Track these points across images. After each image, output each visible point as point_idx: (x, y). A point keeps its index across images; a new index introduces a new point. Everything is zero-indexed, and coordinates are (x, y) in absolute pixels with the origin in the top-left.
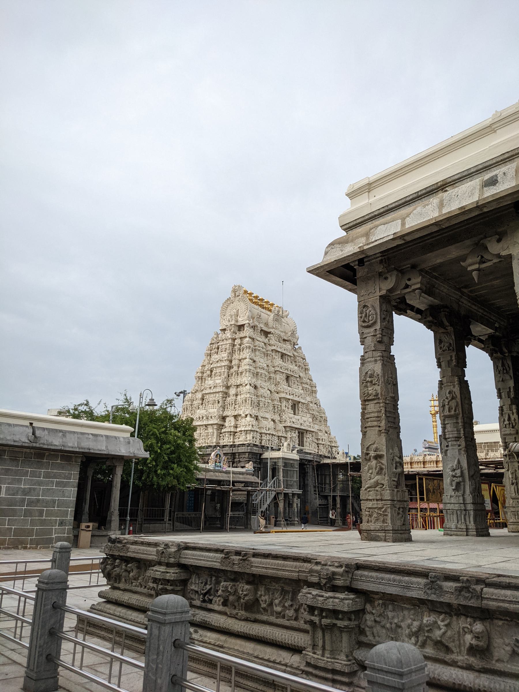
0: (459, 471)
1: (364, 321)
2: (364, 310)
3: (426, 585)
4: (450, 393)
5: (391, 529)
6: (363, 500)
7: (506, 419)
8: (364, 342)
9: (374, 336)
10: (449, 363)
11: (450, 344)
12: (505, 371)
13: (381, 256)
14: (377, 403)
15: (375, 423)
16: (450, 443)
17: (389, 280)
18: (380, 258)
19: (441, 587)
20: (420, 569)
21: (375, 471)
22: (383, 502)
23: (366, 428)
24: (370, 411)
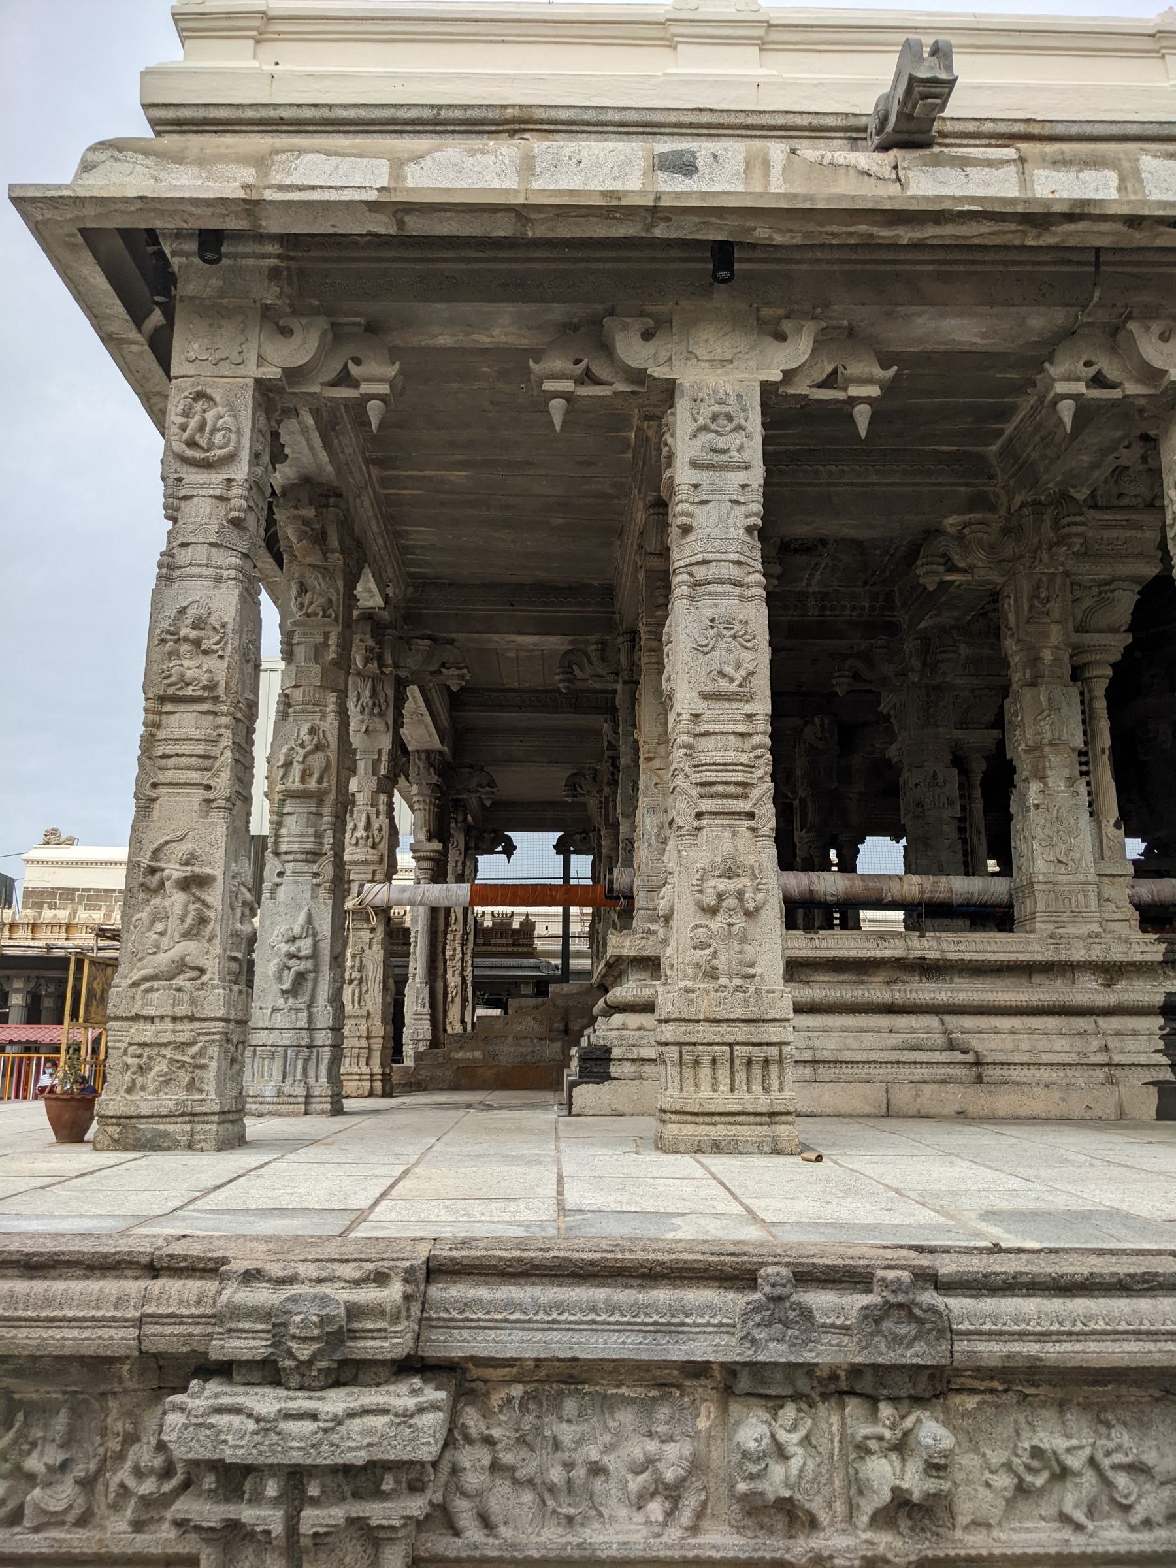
0: (309, 941)
1: (191, 444)
2: (198, 406)
3: (746, 1315)
4: (312, 731)
5: (217, 1108)
6: (117, 1018)
7: (361, 825)
8: (177, 509)
9: (220, 498)
10: (318, 651)
11: (330, 601)
12: (376, 710)
13: (279, 256)
14: (209, 712)
15: (194, 776)
16: (289, 867)
17: (297, 339)
18: (273, 262)
19: (806, 1314)
20: (700, 1257)
21: (174, 926)
22: (198, 1025)
23: (155, 785)
24: (180, 733)
